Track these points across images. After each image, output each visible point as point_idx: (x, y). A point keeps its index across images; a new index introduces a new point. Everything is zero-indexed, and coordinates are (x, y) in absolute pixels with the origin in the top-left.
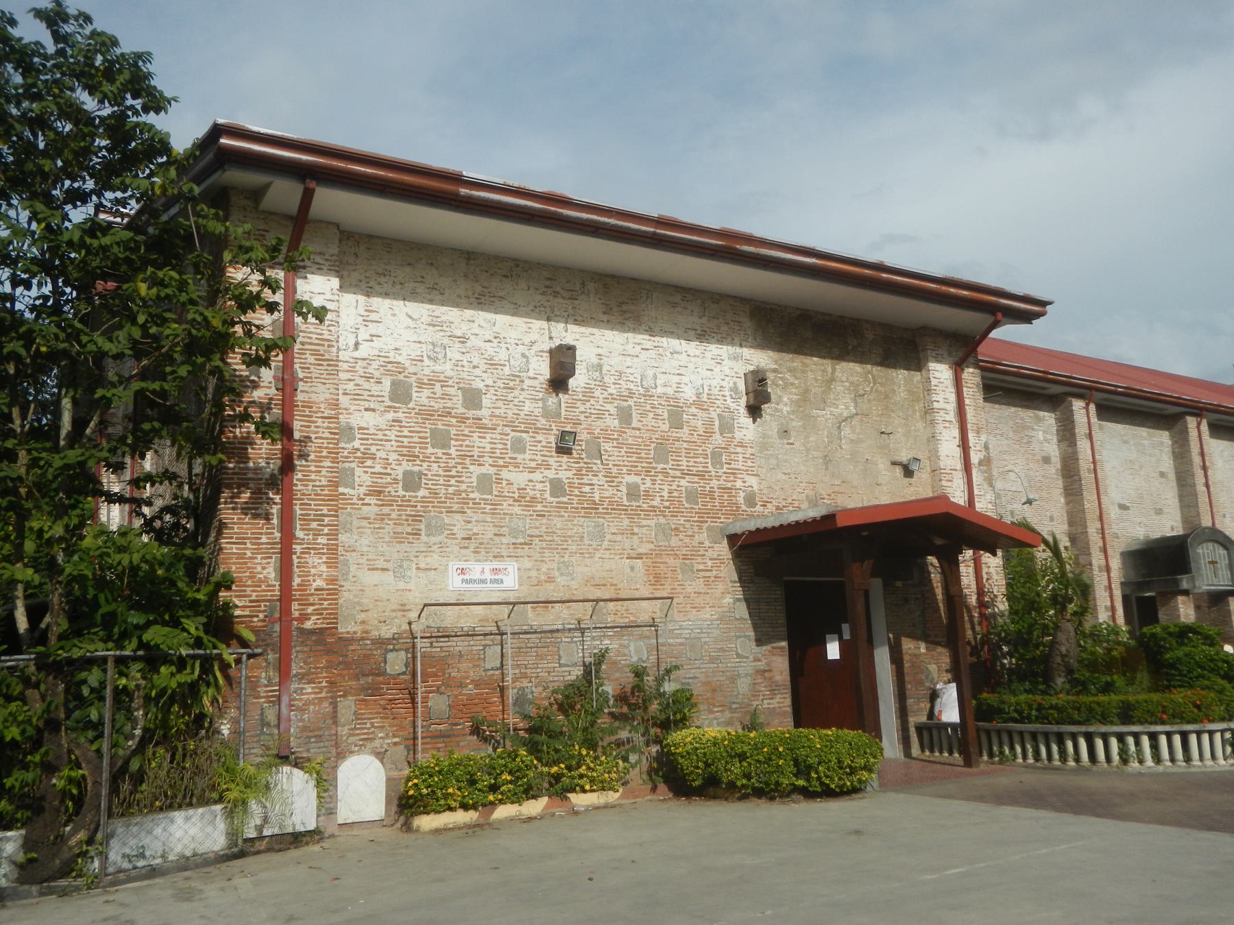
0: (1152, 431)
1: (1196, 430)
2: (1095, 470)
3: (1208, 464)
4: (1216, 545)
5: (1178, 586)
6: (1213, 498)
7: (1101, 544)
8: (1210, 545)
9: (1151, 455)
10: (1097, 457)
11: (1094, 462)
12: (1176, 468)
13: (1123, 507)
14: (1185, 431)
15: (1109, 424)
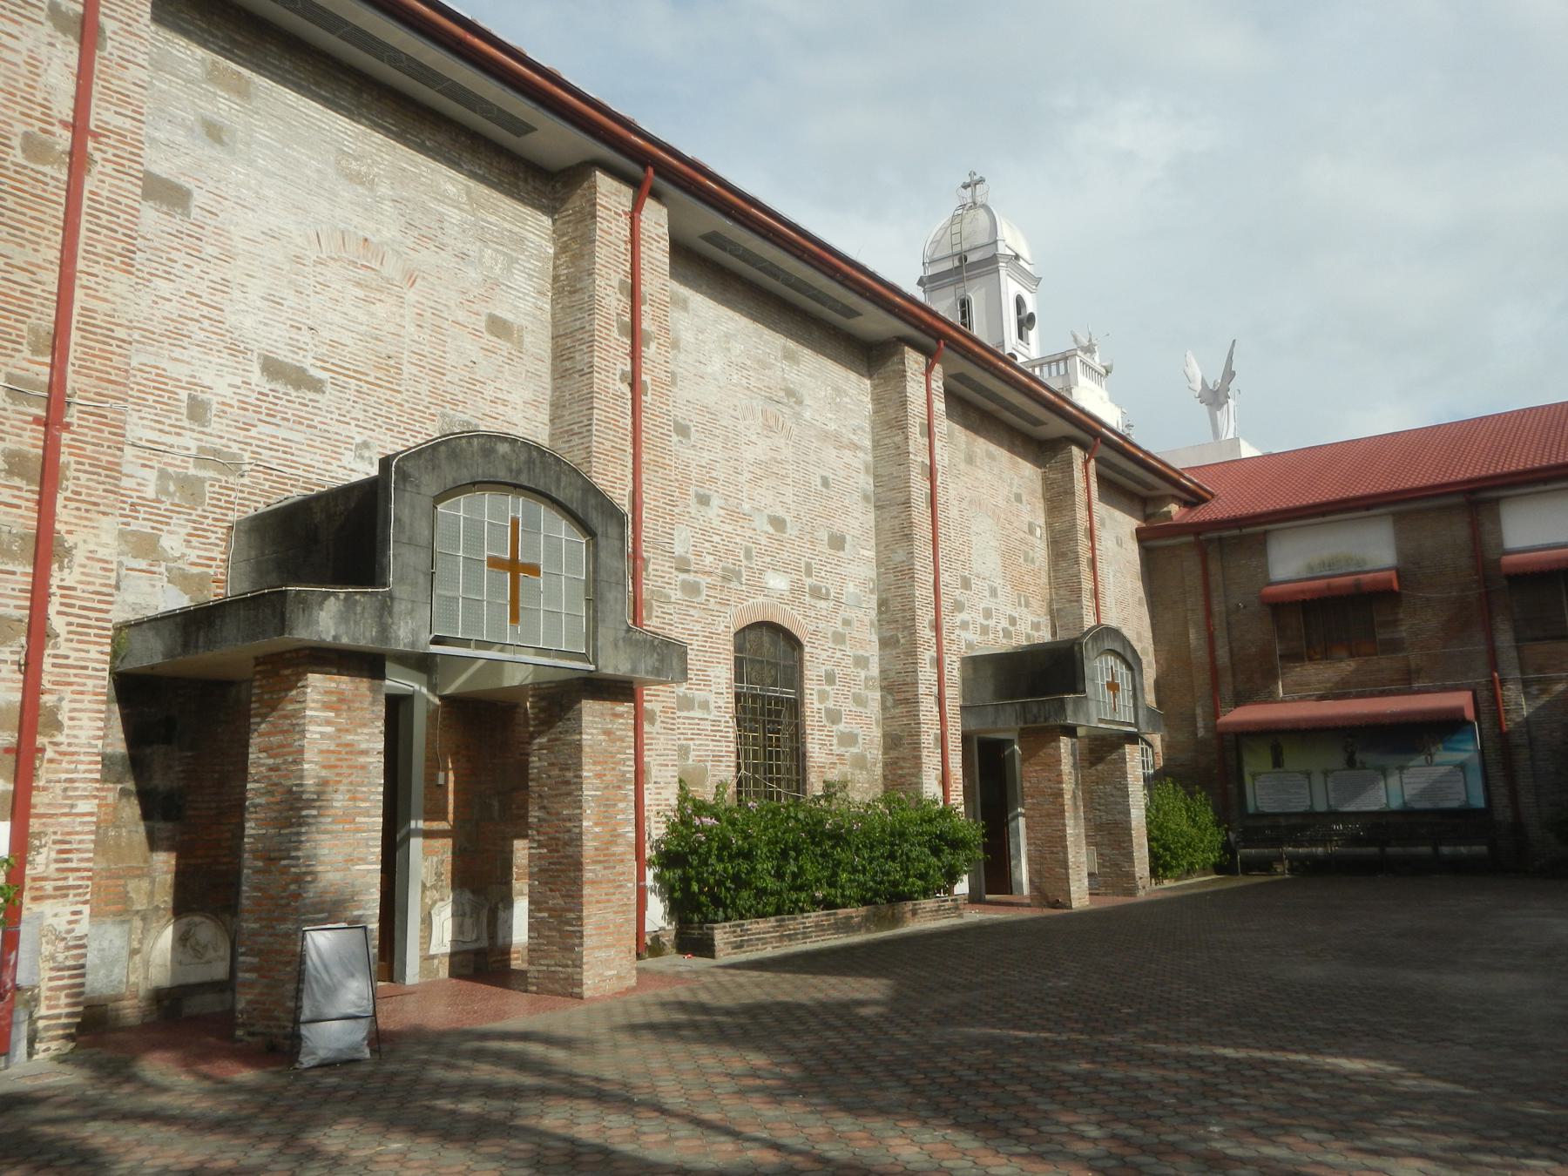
0: (482, 190)
1: (624, 222)
2: (78, 162)
3: (646, 324)
4: (544, 512)
5: (282, 626)
6: (645, 424)
7: (30, 442)
8: (515, 506)
9: (463, 256)
10: (101, 114)
11: (79, 126)
12: (555, 324)
13: (273, 368)
14: (589, 215)
15: (291, 96)
